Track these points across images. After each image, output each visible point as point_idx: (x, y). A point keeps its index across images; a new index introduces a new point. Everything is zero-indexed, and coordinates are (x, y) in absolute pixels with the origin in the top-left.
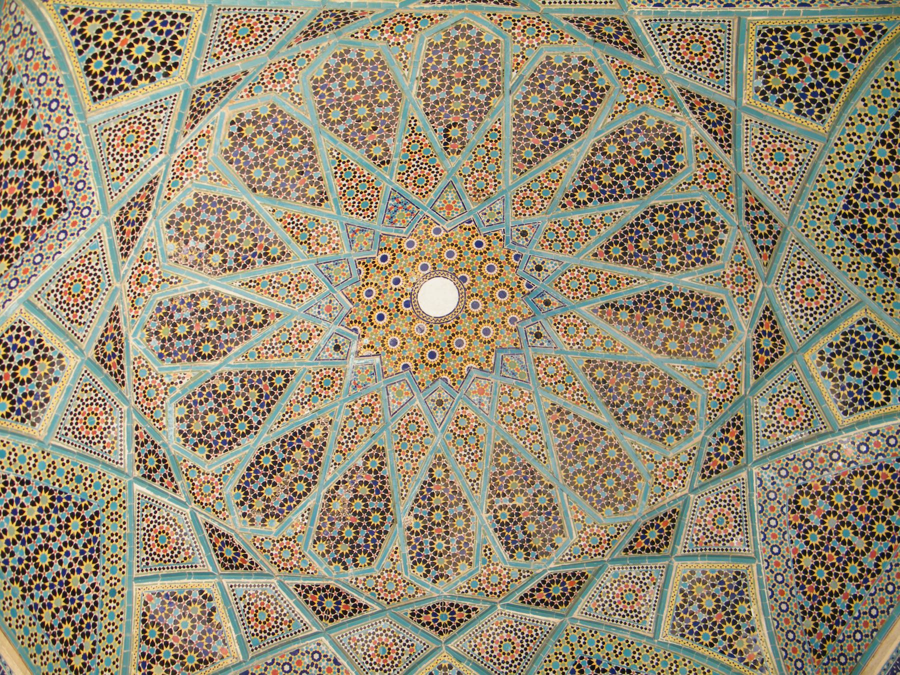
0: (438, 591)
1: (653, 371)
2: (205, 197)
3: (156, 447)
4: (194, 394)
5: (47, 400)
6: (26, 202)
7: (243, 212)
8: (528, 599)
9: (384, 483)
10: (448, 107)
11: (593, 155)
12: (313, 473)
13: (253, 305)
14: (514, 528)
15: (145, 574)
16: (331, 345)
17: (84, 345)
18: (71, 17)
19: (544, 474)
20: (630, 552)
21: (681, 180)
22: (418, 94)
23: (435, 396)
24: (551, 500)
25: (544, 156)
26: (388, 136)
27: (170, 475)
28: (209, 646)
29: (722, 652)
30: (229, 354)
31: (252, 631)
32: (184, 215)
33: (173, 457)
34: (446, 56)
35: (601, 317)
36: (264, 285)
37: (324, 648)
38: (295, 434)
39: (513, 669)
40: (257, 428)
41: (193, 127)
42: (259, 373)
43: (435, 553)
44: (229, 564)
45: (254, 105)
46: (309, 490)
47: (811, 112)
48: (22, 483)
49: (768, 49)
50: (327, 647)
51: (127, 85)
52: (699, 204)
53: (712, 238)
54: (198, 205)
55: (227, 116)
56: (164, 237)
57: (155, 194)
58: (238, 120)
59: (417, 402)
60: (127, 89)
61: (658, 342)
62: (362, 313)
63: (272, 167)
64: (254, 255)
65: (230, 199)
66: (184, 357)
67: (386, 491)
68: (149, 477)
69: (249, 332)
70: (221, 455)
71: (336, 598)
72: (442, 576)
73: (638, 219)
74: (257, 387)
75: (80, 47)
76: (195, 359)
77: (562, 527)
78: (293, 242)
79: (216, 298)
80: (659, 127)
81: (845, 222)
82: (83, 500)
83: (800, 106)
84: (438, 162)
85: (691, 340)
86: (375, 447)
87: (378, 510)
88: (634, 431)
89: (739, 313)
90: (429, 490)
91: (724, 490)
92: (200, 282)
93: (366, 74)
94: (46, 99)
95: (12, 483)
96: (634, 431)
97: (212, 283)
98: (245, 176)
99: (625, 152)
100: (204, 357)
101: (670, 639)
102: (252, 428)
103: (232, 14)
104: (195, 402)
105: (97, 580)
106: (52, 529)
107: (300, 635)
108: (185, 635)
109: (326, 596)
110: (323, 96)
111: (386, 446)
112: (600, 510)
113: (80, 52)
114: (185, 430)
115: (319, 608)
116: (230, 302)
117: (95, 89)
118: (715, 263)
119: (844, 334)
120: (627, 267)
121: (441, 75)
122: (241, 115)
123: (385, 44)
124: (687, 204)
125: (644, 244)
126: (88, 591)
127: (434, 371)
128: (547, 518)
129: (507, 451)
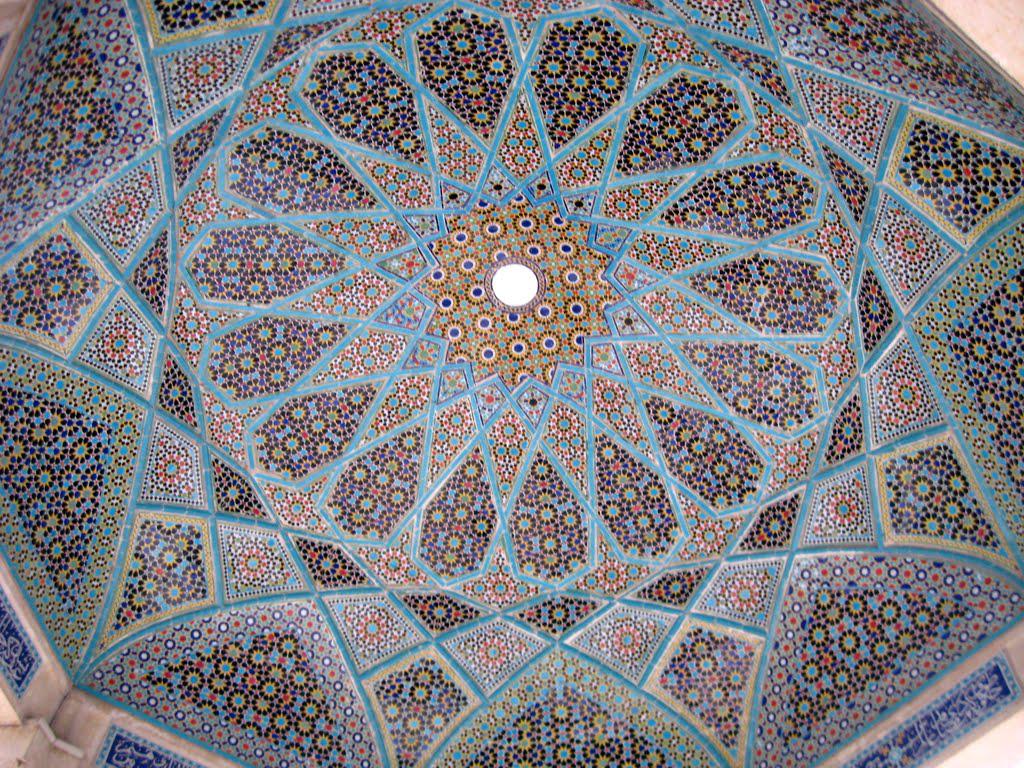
0: (823, 418)
2: (334, 497)
3: (550, 603)
4: (519, 552)
5: (453, 685)
6: (270, 668)
7: (359, 466)
8: (871, 342)
9: (687, 413)
10: (286, 273)
11: (354, 136)
13: (457, 473)
15: (641, 675)
16: (527, 407)
17: (423, 638)
18: (124, 619)
20: (861, 217)
23: (620, 324)
24: (773, 262)
25: (355, 181)
26: (311, 327)
27: (580, 603)
29: (1009, 197)
30: (496, 508)
32: (346, 518)
33: (568, 590)
34: (226, 280)
35: (565, 142)
37: (804, 563)
38: (601, 475)
39: (929, 406)
41: (260, 506)
42: (526, 487)
43: (782, 400)
44: (683, 597)
45: (253, 449)
46: (660, 486)
48: (501, 737)
49: (193, 16)
50: (805, 559)
51: (199, 569)
52: (422, 37)
53: (468, 25)
54: (340, 504)
55: (258, 471)
56: (362, 538)
57: (317, 541)
59: (621, 343)
60: (203, 570)
61: (605, 97)
62: (507, 366)
64: (406, 462)
65: (343, 476)
66: (480, 549)
67: (697, 415)
68: (568, 625)
69: (483, 484)
71: (775, 516)
72: (808, 406)
73: (441, 95)
75: (154, 609)
76: (487, 540)
77: (808, 265)
78: (406, 422)
79: (437, 505)
80: (318, 78)
82: (547, 695)
84: (352, 278)
85: (606, 62)
86: (648, 405)
87: (712, 431)
89: (573, 10)
90: (714, 374)
91: (808, 92)
92: (415, 517)
94: (189, 641)
95: (495, 746)
97: (420, 505)
100: (489, 532)
101: (971, 239)
102: (576, 512)
103: (151, 484)
104: (527, 553)
105: (615, 718)
106: (549, 734)
107: (781, 574)
108: (714, 670)
109: (768, 524)
110: (255, 389)
111: (652, 393)
112: (803, 218)
113: (158, 609)
115: (772, 539)
117: (194, 595)
120: (504, 109)
122: (261, 459)
124: (421, 49)
126: (617, 732)
127: (594, 314)
128: (793, 275)
129: (704, 279)
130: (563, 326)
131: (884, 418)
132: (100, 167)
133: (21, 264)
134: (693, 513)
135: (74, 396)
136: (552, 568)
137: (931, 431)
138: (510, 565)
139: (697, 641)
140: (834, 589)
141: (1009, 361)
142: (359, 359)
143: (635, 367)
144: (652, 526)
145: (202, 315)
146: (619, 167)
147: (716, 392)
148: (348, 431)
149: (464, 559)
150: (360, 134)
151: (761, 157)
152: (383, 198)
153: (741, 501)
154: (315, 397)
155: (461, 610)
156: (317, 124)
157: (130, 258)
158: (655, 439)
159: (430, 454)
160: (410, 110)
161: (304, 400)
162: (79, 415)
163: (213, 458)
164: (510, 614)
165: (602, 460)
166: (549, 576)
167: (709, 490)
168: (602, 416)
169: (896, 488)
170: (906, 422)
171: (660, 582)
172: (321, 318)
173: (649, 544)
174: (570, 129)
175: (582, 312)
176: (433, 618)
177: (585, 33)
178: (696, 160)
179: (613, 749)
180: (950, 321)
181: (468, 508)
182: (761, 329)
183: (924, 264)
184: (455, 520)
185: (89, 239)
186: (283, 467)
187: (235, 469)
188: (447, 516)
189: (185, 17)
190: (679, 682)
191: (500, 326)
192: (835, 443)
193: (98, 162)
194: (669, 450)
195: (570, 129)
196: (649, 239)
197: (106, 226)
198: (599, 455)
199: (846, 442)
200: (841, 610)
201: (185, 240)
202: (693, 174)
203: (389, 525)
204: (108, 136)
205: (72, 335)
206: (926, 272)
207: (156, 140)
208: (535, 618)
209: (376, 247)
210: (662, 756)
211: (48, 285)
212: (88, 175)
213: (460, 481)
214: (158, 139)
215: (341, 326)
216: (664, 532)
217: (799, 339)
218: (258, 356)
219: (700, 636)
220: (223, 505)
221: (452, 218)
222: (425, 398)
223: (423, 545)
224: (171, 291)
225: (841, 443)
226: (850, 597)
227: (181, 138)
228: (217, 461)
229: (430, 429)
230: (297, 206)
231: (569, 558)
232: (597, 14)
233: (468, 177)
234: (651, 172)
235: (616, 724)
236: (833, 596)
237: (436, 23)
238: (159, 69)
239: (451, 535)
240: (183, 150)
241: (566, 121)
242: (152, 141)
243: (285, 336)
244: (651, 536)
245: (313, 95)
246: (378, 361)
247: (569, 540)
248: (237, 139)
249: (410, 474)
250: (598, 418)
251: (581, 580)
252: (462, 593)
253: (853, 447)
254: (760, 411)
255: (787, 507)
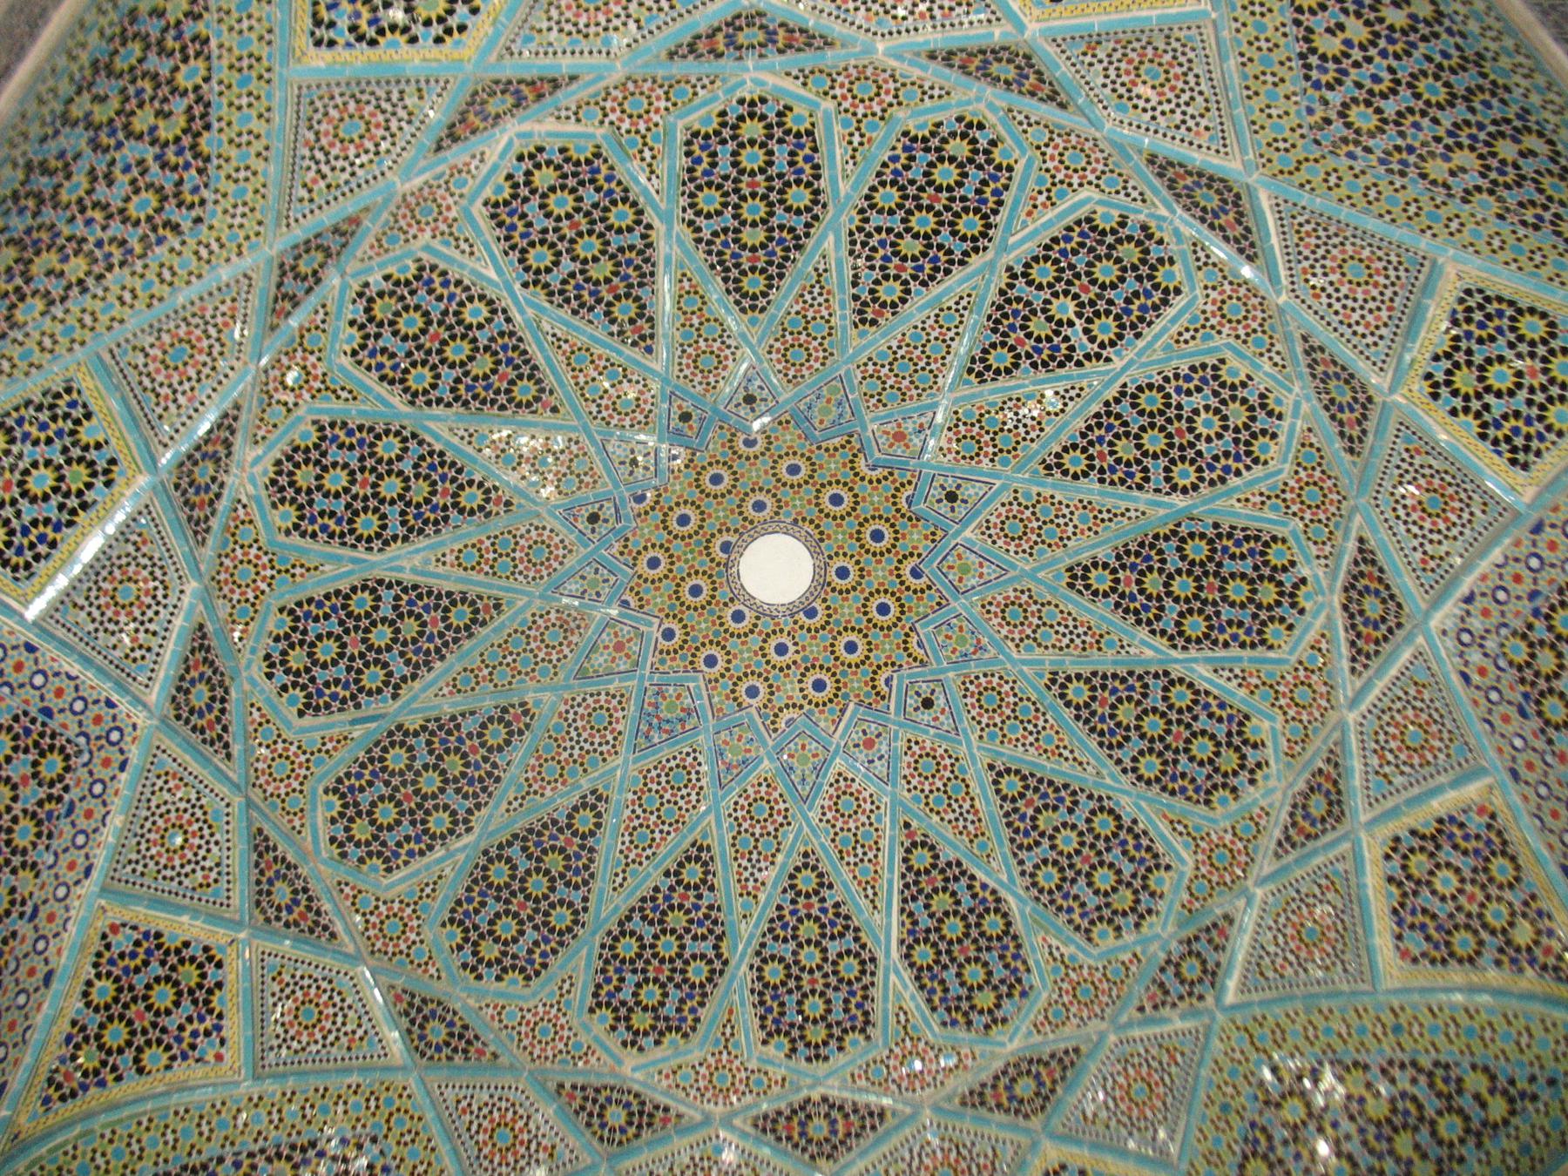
0: (1297, 405)
1: (690, 214)
2: (763, 1027)
3: (1168, 962)
4: (1070, 921)
7: (764, 961)
8: (1247, 247)
9: (1128, 553)
10: (464, 775)
11: (395, 538)
12: (1150, 681)
13: (903, 876)
14: (1120, 302)
16: (925, 716)
19: (994, 290)
20: (1063, 97)
21: (340, 405)
22: (468, 830)
23: (944, 507)
24: (1036, 259)
25: (449, 594)
26: (555, 822)
27: (1208, 930)
28: (1478, 837)
30: (992, 884)
31: (1441, 756)
34: (391, 839)
35: (652, 336)
36: (865, 872)
37: (1450, 624)
38: (1092, 730)
40: (1100, 799)
41: (666, 1109)
42: (1009, 825)
43: (1225, 428)
45: (603, 1036)
46: (1181, 680)
47: (73, 404)
49: (42, 538)
50: (1446, 615)
52: (354, 353)
54: (778, 1032)
56: (842, 1059)
57: (783, 1106)
58: (633, 1043)
59: (967, 533)
61: (635, 239)
63: (679, 956)
64: (824, 910)
67: (1142, 545)
69: (949, 864)
70: (1159, 847)
72: (1263, 406)
73: (449, 405)
74: (1033, 819)
76: (1015, 937)
77: (1078, 223)
80: (282, 501)
81: (184, 218)
83: (77, 422)
84: (556, 720)
85: (589, 196)
86: (1071, 586)
87: (1179, 549)
88: (823, 184)
90: (1113, 470)
93: (482, 920)
96: (823, 184)
98: (708, 988)
99: (358, 505)
100: (1009, 924)
104: (1082, 916)
107: (1434, 667)
108: (1462, 881)
109: (1361, 612)
110: (544, 955)
111: (1062, 566)
112: (1010, 169)
114: (1132, 918)
115: (1383, 627)
116: (911, 914)
118: (428, 259)
119: (373, 43)
120: (539, 360)
121: (424, 822)
122: (624, 1044)
123: (425, 928)
124: (369, 368)
125: (483, 364)
126: (1393, 1081)
128: (1075, 252)
130: (880, 573)
131: (1360, 329)
132: (91, 803)
133: (86, 994)
134: (1254, 681)
135: (288, 1121)
136: (1133, 910)
137: (1428, 289)
138: (1072, 949)
139: (1405, 857)
140: (1518, 624)
141: (1405, 92)
142: (653, 818)
143: (1012, 548)
144: (1218, 744)
145: (396, 906)
146: (743, 310)
147: (1136, 493)
148: (713, 926)
149: (1004, 989)
150: (401, 531)
151: (882, 144)
152: (508, 590)
153: (1302, 612)
154: (632, 910)
155: (1054, 1064)
156: (338, 559)
157: (240, 895)
158: (1120, 622)
159: (848, 877)
160: (431, 454)
161: (621, 924)
162: (313, 1144)
163: (552, 1086)
164: (1124, 1019)
165: (1078, 707)
166: (1137, 925)
167: (1248, 632)
168: (1029, 649)
169: (1466, 410)
170: (1390, 309)
171: (1292, 815)
172: (560, 800)
173: (1235, 773)
174: (641, 316)
175: (888, 535)
176: (1021, 1101)
177: (527, 183)
178: (816, 218)
179: (1406, 1113)
180: (1293, 120)
181: (956, 913)
182: (1108, 360)
183: (1191, 78)
184: (951, 942)
185: (156, 903)
186: (662, 1034)
187: (597, 1083)
188: (934, 945)
189: (32, 546)
190: (1428, 938)
191: (804, 638)
192: (1341, 423)
193: (82, 799)
194: (1149, 623)
195: (641, 316)
196: (870, 368)
197: (169, 873)
198: (1068, 704)
199: (1352, 410)
200: (1553, 647)
201: (297, 823)
202: (831, 238)
203: (866, 1014)
204: (67, 758)
205: (229, 1043)
206: (1203, 87)
207: (139, 722)
208: (1161, 997)
209: (554, 657)
210: (1486, 1069)
211: (146, 998)
212: (82, 823)
213: (916, 883)
214: (140, 718)
215: (593, 792)
216: (1238, 738)
217: (1165, 330)
218: (514, 908)
219: (1403, 849)
220: (611, 1141)
221: (617, 547)
222: (782, 806)
223: (934, 1009)
224: (332, 901)
225: (1346, 416)
226: (1548, 617)
227: (174, 699)
228: (561, 1086)
229: (822, 844)
230: (404, 679)
231: (1144, 878)
232: (517, 148)
233: (587, 479)
234: (786, 282)
235: (1384, 1071)
236: (1524, 637)
237: (352, 323)
238: (61, 633)
239: (961, 966)
240: (192, 712)
241: (624, 310)
242: (134, 727)
243: (529, 857)
244: (1229, 760)
245: (296, 527)
246: (681, 803)
247: (1125, 853)
248: (253, 651)
249: (840, 923)
250: (1025, 656)
251: (1186, 896)
252: (1039, 1038)
253: (1364, 406)
254: (1212, 468)
255: (1363, 567)
